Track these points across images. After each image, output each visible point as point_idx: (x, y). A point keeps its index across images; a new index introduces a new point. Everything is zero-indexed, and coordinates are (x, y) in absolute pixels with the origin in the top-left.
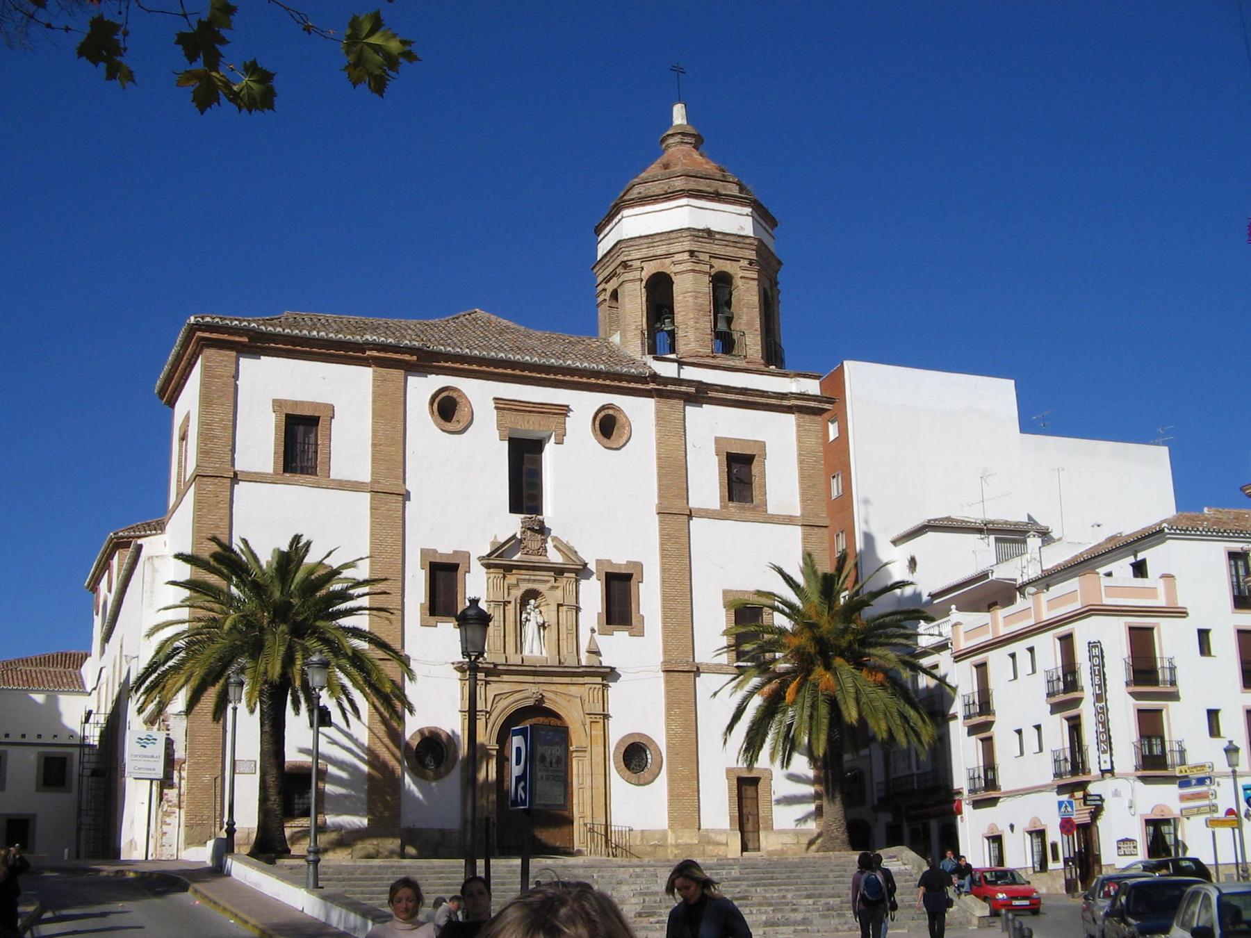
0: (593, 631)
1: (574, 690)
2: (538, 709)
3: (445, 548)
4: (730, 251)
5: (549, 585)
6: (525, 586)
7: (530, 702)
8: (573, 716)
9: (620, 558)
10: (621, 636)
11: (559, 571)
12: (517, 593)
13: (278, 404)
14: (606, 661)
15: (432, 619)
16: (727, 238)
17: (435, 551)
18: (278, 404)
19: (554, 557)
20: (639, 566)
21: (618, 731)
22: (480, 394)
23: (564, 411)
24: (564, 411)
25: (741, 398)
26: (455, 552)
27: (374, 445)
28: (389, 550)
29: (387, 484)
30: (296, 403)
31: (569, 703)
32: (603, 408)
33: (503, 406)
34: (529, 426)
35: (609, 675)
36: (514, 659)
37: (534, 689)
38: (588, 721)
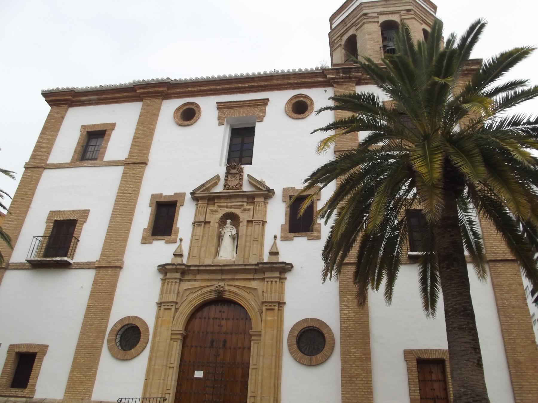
0: (275, 237)
1: (254, 284)
2: (220, 300)
3: (168, 191)
5: (243, 208)
7: (213, 296)
8: (250, 303)
10: (301, 242)
11: (251, 198)
12: (218, 216)
15: (150, 238)
17: (161, 195)
21: (292, 316)
24: (264, 102)
26: (176, 194)
27: (134, 139)
28: (128, 196)
29: (136, 159)
30: (94, 125)
31: (249, 293)
32: (295, 97)
33: (221, 106)
34: (241, 116)
35: (286, 268)
36: (208, 262)
37: (221, 284)
38: (264, 308)
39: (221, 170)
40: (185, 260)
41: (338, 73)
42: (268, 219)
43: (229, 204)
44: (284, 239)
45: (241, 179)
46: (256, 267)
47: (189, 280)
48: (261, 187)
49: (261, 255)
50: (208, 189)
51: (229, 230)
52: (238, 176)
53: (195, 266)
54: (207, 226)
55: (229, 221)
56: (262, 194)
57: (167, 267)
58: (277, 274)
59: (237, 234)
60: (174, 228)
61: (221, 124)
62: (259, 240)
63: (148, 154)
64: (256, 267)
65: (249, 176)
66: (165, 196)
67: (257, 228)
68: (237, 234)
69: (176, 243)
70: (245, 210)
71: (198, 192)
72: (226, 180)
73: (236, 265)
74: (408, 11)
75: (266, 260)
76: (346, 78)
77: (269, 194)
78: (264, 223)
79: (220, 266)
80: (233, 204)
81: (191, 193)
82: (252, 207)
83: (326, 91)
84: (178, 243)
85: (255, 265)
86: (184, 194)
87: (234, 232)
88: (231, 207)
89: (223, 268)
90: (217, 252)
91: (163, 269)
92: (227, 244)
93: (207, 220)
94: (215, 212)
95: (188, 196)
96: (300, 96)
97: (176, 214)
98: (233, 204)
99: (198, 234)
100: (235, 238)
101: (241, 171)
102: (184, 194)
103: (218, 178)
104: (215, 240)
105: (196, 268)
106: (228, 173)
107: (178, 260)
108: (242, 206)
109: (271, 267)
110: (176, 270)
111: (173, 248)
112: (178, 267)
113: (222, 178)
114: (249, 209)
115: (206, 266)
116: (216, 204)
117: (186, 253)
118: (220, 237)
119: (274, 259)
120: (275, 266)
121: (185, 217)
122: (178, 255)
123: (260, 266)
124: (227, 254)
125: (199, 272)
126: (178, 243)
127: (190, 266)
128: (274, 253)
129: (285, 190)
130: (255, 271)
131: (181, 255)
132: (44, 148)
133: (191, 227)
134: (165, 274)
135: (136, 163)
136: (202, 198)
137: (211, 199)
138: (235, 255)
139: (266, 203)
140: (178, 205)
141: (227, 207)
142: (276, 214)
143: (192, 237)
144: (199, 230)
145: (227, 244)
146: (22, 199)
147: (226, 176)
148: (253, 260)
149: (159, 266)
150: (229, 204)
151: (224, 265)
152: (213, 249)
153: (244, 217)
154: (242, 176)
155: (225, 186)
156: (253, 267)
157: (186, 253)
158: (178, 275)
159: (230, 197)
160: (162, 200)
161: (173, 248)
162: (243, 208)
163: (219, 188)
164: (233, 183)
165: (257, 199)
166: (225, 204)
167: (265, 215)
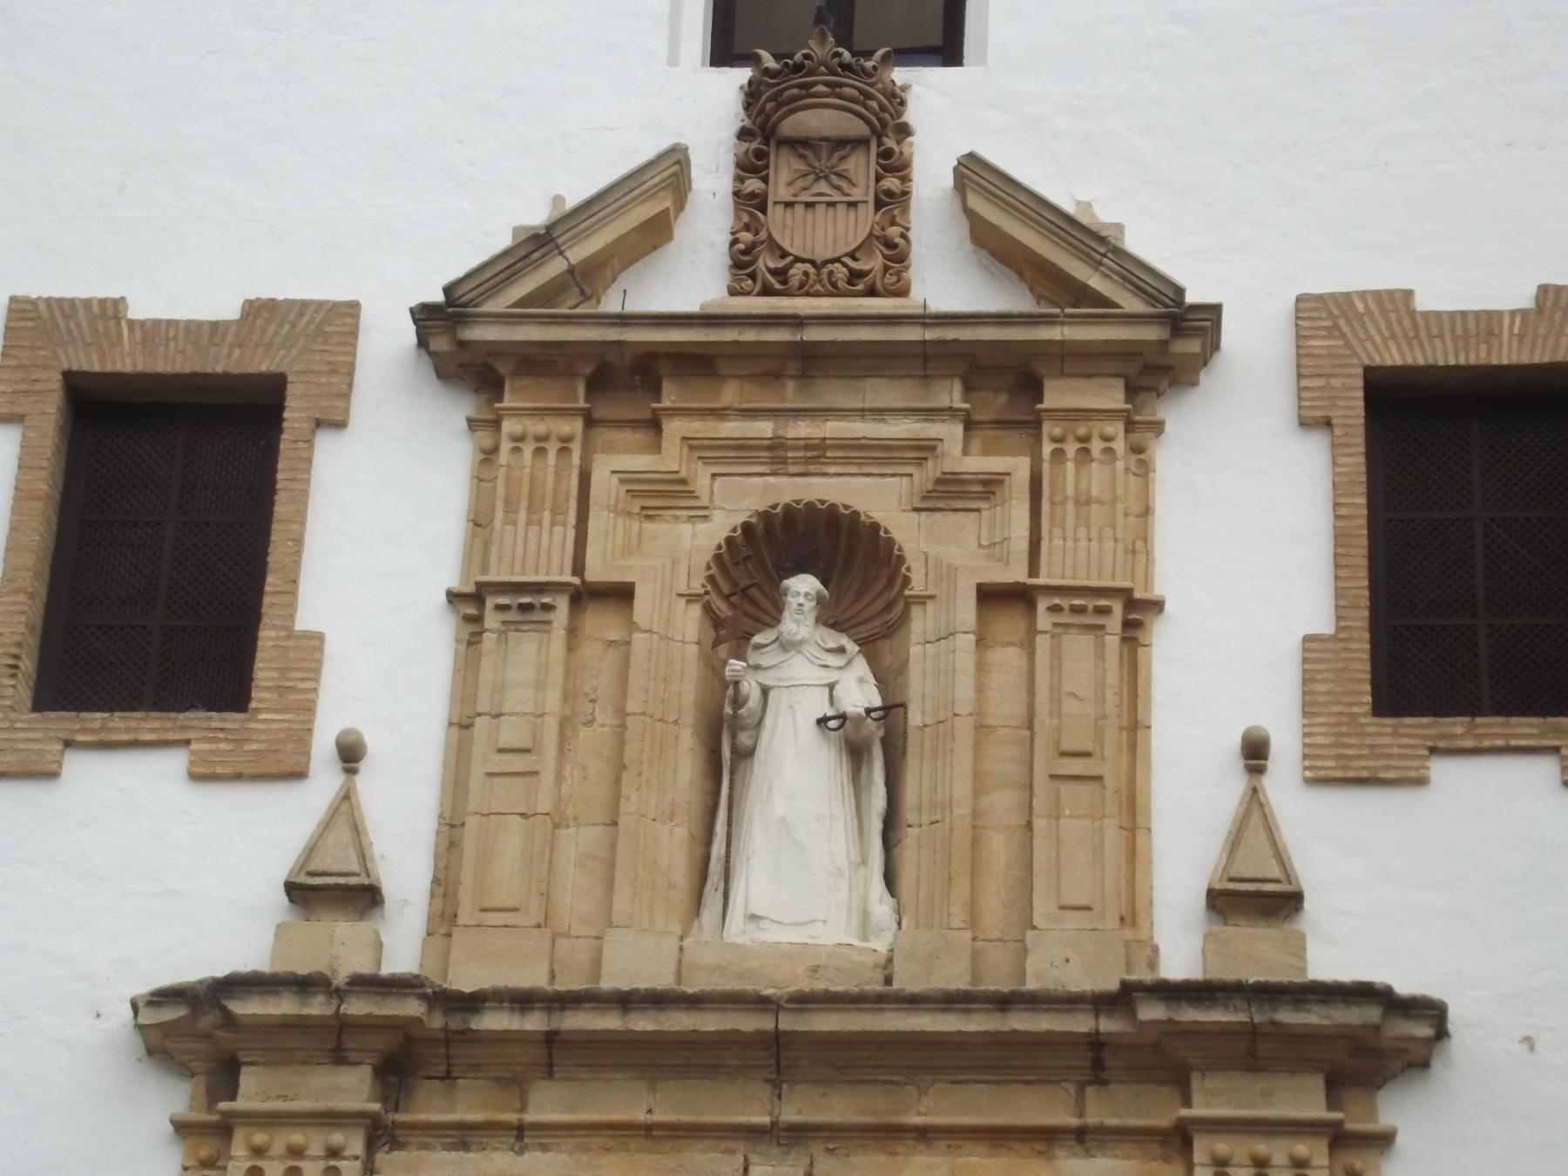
0: (1255, 752)
3: (181, 280)
5: (932, 470)
6: (739, 499)
11: (1001, 378)
12: (696, 540)
14: (1339, 945)
17: (111, 310)
19: (946, 280)
26: (257, 310)
35: (1379, 1041)
36: (638, 961)
39: (706, 108)
40: (401, 943)
42: (1170, 578)
43: (801, 429)
44: (1334, 772)
45: (892, 202)
46: (1109, 1025)
47: (463, 1136)
48: (1096, 282)
49: (1133, 914)
50: (588, 278)
51: (808, 676)
52: (860, 166)
53: (523, 1000)
54: (601, 623)
55: (803, 586)
56: (1094, 341)
57: (247, 1008)
58: (1305, 1100)
59: (891, 710)
60: (267, 637)
62: (1108, 768)
64: (1109, 1025)
65: (973, 174)
66: (154, 331)
67: (1081, 662)
68: (891, 710)
69: (298, 774)
70: (951, 493)
71: (499, 304)
72: (751, 204)
73: (914, 1001)
75: (1180, 951)
77: (1170, 343)
78: (1138, 612)
79: (762, 1003)
80: (833, 428)
81: (424, 316)
82: (1018, 467)
84: (324, 781)
85: (1101, 1003)
86: (336, 323)
87: (858, 692)
88: (817, 455)
89: (787, 1023)
90: (708, 873)
91: (200, 1032)
92: (799, 792)
93: (597, 571)
94: (661, 497)
95: (387, 338)
97: (281, 508)
98: (833, 428)
99: (519, 699)
100: (874, 745)
101: (885, 130)
102: (336, 323)
103: (670, 173)
104: (686, 765)
105: (534, 1022)
106: (762, 138)
107: (341, 947)
108: (924, 450)
109: (1252, 1032)
110: (334, 1042)
111: (271, 829)
112: (356, 1007)
113: (713, 181)
114: (991, 485)
115: (625, 1001)
116: (674, 428)
117: (405, 872)
118: (726, 742)
119: (1255, 955)
120: (1288, 1016)
121: (378, 532)
122: (332, 891)
123: (1151, 1012)
124: (804, 888)
125: (555, 1054)
126: (324, 781)
127: (474, 1002)
128: (1257, 899)
129: (1319, 317)
130: (1095, 1061)
131: (363, 897)
133: (438, 637)
134: (223, 1075)
136: (538, 362)
137: (631, 376)
138: (881, 907)
139: (1141, 431)
140: (294, 415)
141: (776, 454)
142: (1247, 539)
143: (462, 725)
144: (529, 662)
145: (799, 792)
147: (751, 165)
148: (1066, 960)
149: (164, 996)
150: (801, 429)
151: (803, 1001)
152: (672, 846)
153: (947, 555)
154: (895, 165)
155: (742, 262)
156: (1081, 1023)
157: (405, 872)
158: (353, 1088)
159: (812, 362)
160: (127, 360)
161: (271, 829)
162: (932, 470)
163: (688, 278)
164: (823, 233)
165: (1058, 394)
166: (764, 429)
167: (1139, 545)
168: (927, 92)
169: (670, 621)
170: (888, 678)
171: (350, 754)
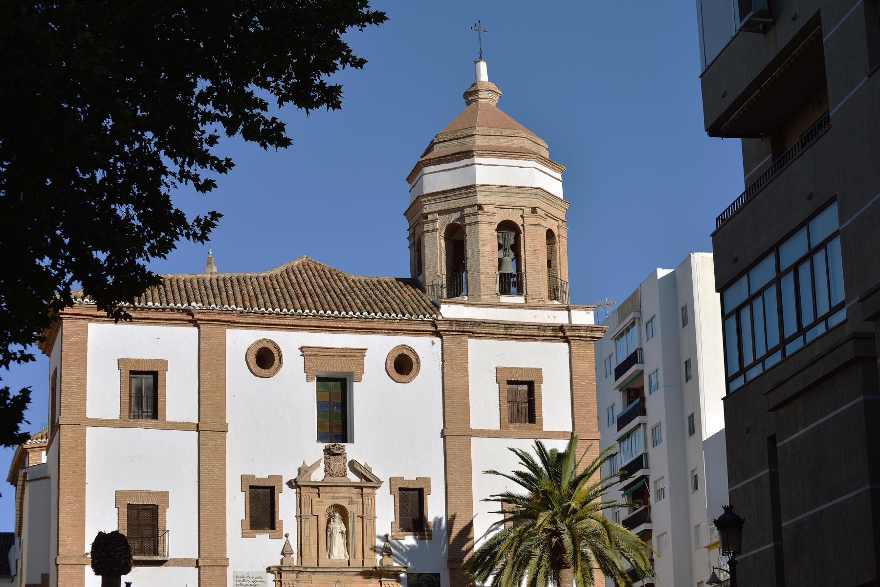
3: (262, 473)
4: (514, 201)
6: (329, 502)
9: (410, 475)
13: (121, 363)
16: (510, 190)
18: (121, 363)
20: (427, 480)
22: (290, 342)
23: (362, 352)
24: (362, 352)
25: (519, 332)
30: (138, 361)
32: (397, 348)
34: (335, 368)
41: (451, 325)
51: (338, 526)
56: (367, 481)
61: (308, 379)
63: (224, 417)
66: (259, 479)
74: (534, 210)
76: (459, 331)
83: (433, 343)
92: (339, 541)
96: (405, 347)
100: (346, 534)
111: (279, 544)
121: (287, 504)
122: (285, 552)
132: (76, 394)
135: (210, 428)
145: (339, 541)
146: (74, 472)
161: (279, 544)
168: (348, 446)
169: (323, 520)
170: (346, 524)
171: (286, 536)
